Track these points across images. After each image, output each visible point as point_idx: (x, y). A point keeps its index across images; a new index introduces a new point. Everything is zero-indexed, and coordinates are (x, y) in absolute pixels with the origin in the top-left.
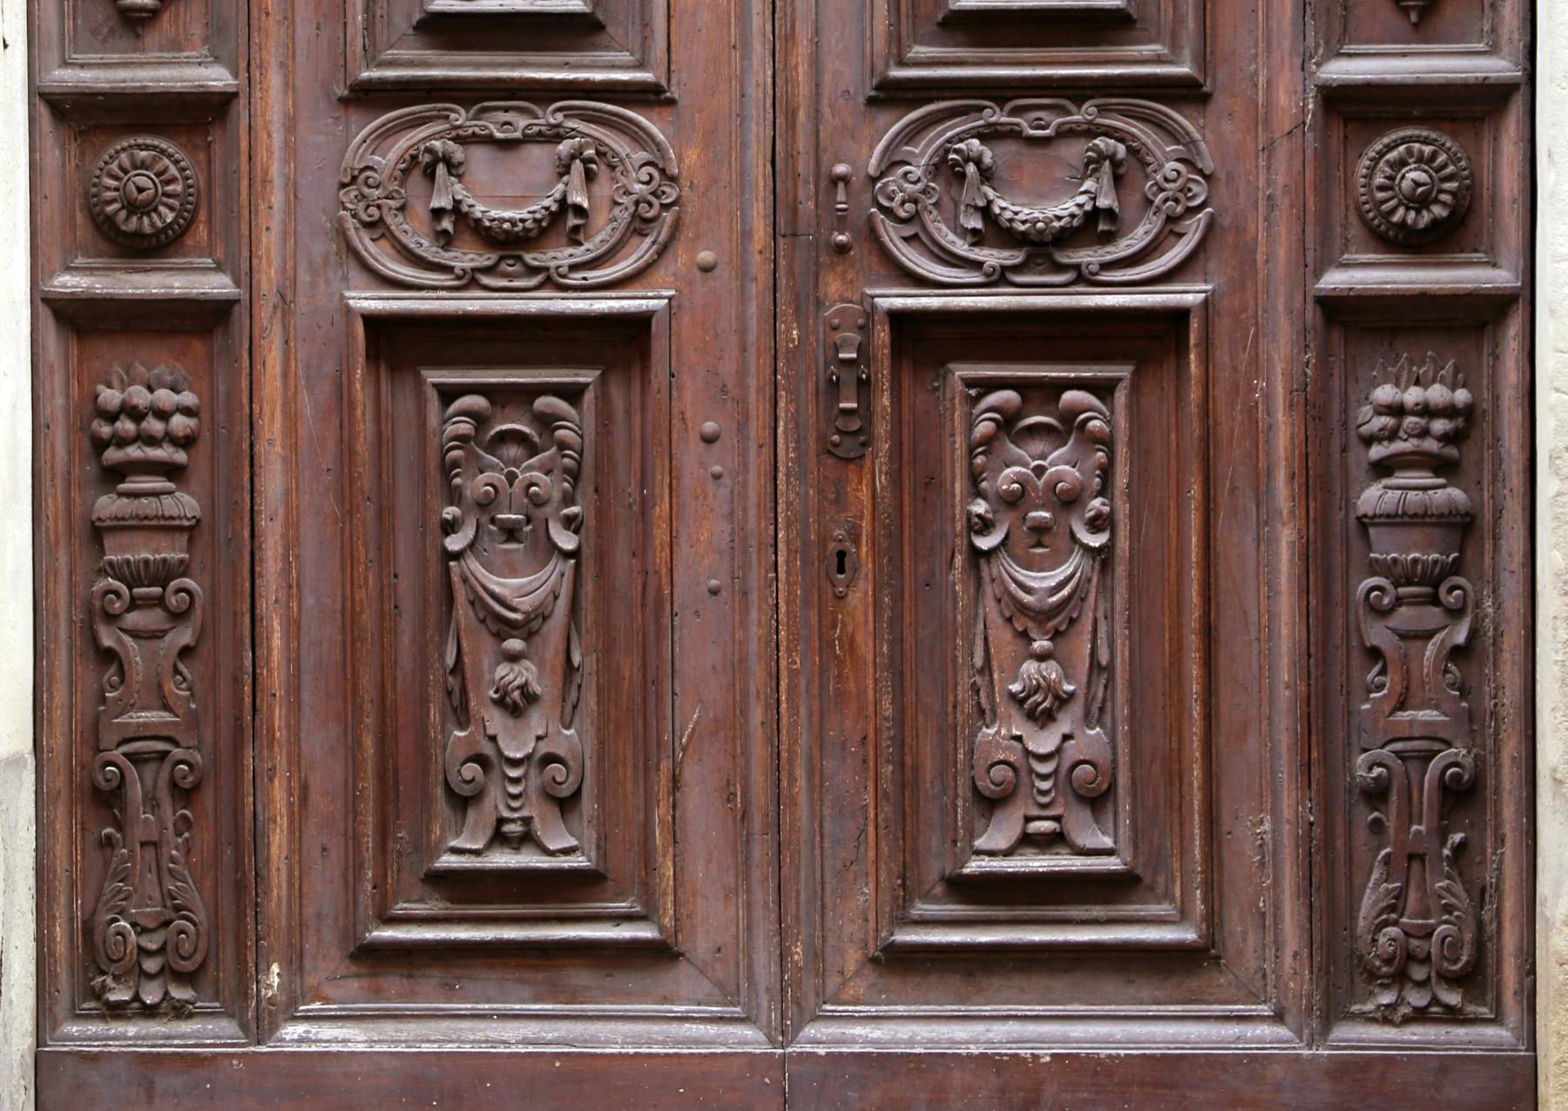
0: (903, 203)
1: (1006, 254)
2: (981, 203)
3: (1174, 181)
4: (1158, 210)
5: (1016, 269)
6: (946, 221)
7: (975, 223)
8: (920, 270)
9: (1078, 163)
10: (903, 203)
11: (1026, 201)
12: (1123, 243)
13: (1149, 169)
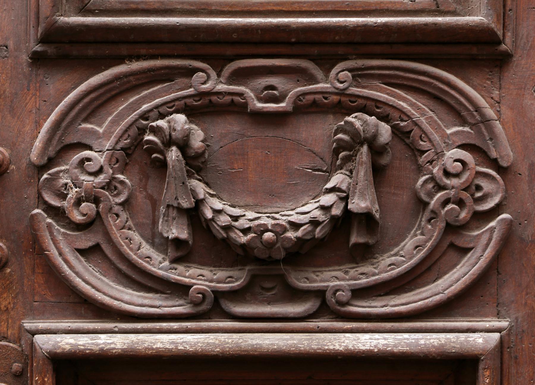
0: (78, 202)
1: (221, 274)
2: (186, 204)
3: (457, 175)
4: (434, 215)
5: (236, 295)
6: (139, 227)
7: (178, 231)
8: (99, 296)
9: (323, 147)
10: (78, 202)
11: (250, 201)
12: (386, 260)
13: (422, 159)
